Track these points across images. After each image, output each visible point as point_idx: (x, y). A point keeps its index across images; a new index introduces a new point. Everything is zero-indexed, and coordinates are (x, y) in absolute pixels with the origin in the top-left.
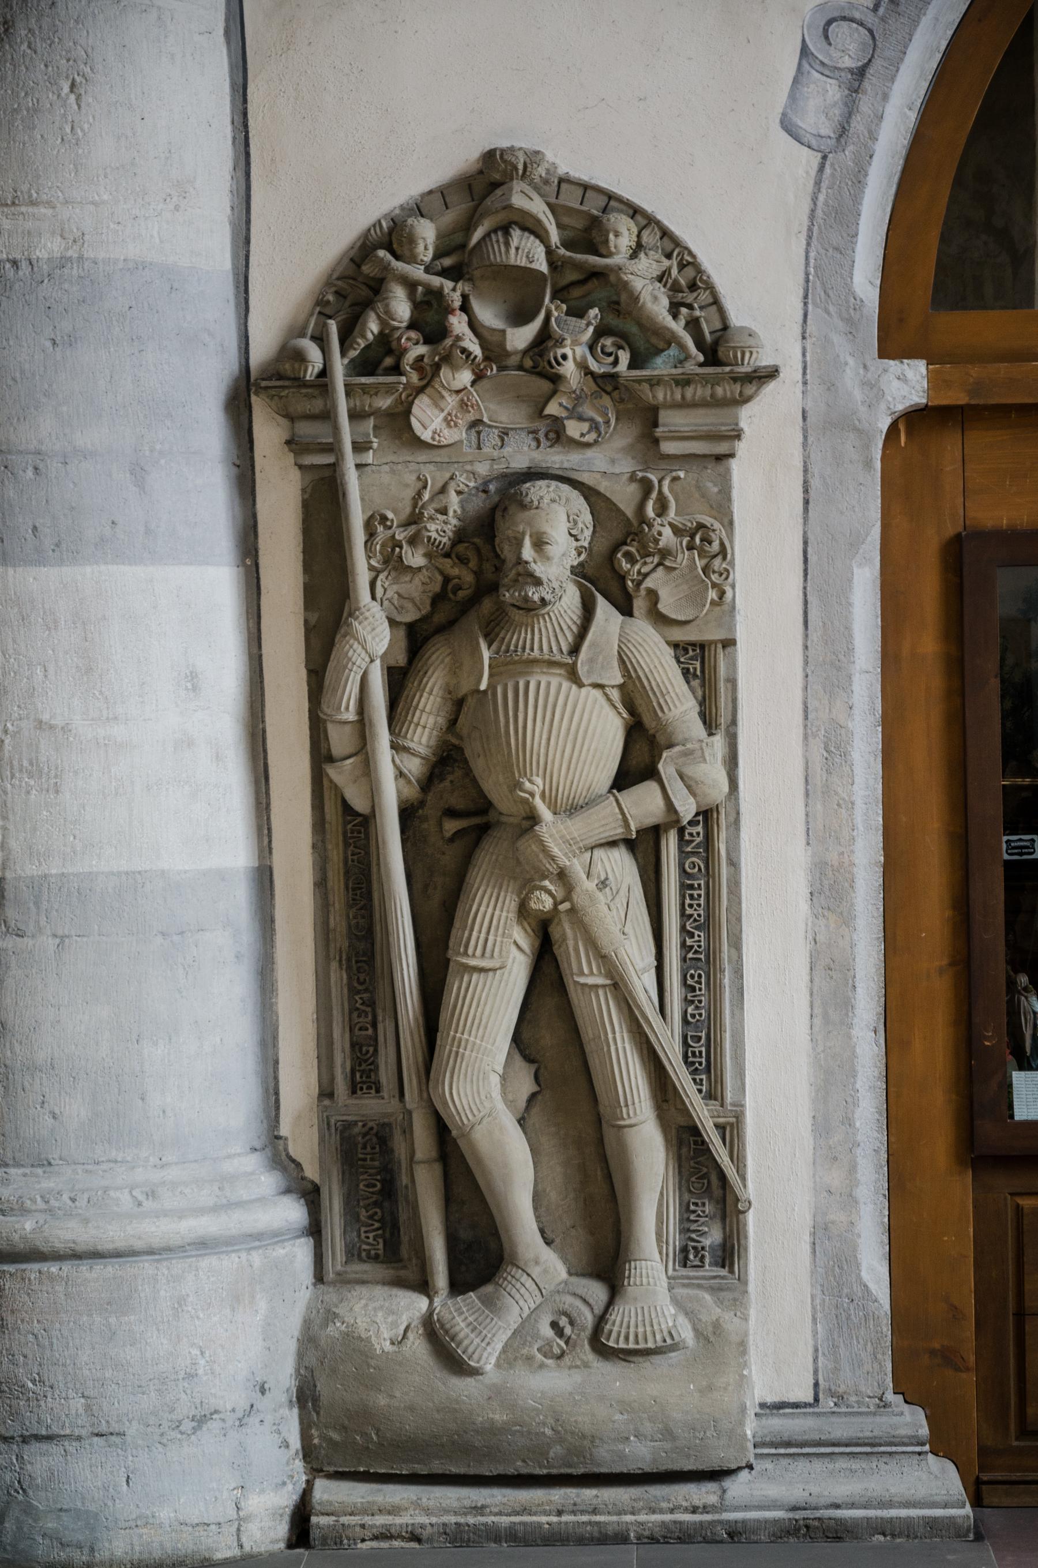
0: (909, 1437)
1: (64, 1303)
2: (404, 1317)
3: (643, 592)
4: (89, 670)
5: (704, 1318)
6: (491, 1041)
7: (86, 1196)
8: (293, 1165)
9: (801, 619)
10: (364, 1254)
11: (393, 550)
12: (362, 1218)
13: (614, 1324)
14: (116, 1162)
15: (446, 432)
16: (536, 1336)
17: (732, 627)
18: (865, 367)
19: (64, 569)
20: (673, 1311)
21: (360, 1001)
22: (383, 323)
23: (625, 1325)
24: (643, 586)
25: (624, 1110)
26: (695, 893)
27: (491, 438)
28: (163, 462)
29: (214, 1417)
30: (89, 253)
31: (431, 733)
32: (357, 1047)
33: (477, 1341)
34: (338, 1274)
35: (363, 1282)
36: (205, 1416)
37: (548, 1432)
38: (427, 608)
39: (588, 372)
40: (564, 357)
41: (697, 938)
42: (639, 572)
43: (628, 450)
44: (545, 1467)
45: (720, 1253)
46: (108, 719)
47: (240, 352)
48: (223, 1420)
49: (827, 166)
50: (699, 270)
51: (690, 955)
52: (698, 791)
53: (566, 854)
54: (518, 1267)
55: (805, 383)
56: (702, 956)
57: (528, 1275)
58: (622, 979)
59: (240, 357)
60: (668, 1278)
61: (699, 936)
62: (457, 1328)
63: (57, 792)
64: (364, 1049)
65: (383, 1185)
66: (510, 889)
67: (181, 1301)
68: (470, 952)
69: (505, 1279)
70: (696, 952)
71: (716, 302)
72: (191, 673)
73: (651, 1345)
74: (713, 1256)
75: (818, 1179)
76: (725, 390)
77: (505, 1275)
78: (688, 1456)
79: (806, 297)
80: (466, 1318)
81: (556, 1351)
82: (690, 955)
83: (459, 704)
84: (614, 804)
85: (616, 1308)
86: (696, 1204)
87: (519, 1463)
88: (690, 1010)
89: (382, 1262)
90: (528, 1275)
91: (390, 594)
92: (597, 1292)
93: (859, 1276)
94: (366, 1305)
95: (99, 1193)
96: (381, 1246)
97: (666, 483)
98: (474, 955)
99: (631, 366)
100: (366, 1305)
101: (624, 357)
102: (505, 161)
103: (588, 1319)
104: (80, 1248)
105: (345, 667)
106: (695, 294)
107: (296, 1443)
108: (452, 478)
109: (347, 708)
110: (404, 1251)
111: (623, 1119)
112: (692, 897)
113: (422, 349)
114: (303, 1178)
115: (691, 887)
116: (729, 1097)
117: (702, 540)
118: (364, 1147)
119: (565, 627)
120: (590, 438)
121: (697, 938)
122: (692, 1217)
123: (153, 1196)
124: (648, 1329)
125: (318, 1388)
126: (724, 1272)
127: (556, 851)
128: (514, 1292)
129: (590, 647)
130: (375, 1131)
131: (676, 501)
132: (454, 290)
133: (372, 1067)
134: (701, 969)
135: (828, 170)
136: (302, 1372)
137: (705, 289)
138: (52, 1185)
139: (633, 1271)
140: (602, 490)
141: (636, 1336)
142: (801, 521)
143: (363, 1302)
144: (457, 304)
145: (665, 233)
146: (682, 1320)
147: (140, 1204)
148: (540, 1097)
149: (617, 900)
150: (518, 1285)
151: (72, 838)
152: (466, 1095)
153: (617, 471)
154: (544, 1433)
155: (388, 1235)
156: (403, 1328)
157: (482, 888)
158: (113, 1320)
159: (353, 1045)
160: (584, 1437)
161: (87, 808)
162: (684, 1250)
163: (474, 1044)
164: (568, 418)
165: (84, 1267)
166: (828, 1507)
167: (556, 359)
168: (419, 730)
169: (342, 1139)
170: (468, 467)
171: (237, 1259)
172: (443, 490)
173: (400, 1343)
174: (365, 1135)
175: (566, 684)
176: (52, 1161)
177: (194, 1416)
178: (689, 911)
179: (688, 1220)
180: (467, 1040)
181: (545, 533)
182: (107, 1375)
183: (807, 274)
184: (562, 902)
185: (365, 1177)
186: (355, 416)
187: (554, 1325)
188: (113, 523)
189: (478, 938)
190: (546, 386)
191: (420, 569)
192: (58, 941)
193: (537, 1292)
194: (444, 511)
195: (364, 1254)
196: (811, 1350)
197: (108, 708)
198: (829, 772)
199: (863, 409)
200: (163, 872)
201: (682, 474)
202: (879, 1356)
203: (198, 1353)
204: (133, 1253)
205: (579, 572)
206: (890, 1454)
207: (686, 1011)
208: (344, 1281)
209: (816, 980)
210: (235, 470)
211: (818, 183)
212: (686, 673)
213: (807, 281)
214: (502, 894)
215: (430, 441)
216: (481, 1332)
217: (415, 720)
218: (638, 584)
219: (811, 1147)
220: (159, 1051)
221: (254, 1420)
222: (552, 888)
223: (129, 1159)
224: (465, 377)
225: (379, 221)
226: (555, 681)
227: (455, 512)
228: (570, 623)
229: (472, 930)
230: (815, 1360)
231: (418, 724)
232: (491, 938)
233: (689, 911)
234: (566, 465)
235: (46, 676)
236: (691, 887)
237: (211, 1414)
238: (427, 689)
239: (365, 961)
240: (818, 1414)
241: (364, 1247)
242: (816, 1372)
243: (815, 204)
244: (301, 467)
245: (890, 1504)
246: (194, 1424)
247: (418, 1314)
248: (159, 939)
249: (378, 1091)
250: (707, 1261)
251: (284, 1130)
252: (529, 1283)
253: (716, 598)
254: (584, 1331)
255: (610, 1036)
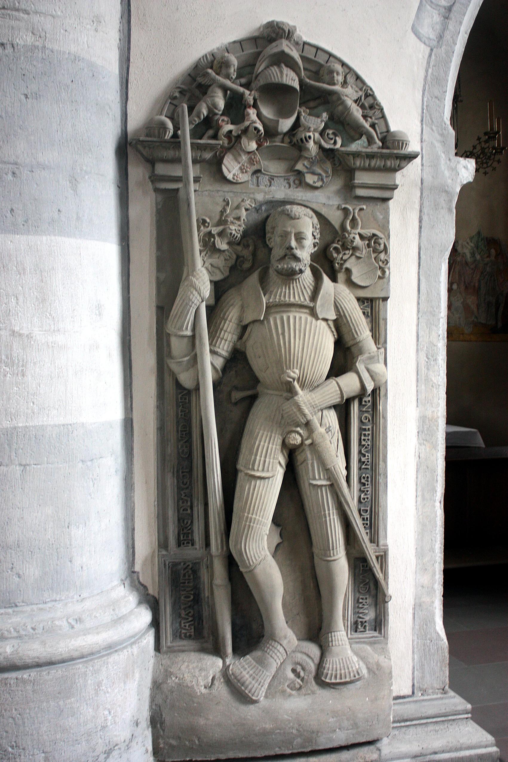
0: (463, 710)
1: (32, 696)
2: (211, 672)
3: (343, 270)
4: (44, 300)
5: (371, 660)
6: (267, 518)
7: (41, 625)
8: (142, 588)
9: (417, 289)
10: (183, 635)
11: (210, 240)
12: (183, 615)
13: (328, 670)
14: (56, 601)
15: (241, 175)
16: (286, 679)
17: (388, 291)
18: (449, 160)
19: (30, 237)
20: (356, 659)
21: (183, 495)
22: (210, 111)
23: (334, 669)
24: (344, 266)
25: (332, 552)
26: (367, 433)
27: (264, 180)
28: (87, 177)
29: (116, 748)
30: (49, 45)
31: (229, 344)
32: (181, 521)
33: (256, 685)
34: (169, 647)
35: (183, 651)
36: (111, 749)
37: (294, 731)
38: (227, 273)
39: (321, 147)
40: (310, 137)
41: (367, 457)
42: (342, 258)
43: (338, 192)
44: (291, 750)
45: (373, 624)
46: (54, 330)
47: (122, 122)
48: (120, 749)
49: (433, 54)
50: (375, 98)
51: (363, 467)
52: (376, 379)
53: (311, 413)
54: (275, 641)
55: (422, 165)
56: (369, 467)
57: (281, 645)
58: (336, 481)
59: (122, 125)
60: (349, 639)
61: (368, 456)
62: (245, 679)
63: (23, 375)
64: (185, 522)
65: (194, 597)
66: (277, 432)
67: (99, 684)
68: (256, 468)
69: (269, 648)
70: (366, 465)
71: (383, 117)
72: (98, 305)
73: (348, 679)
74: (370, 625)
75: (417, 581)
76: (391, 164)
77: (268, 645)
78: (363, 736)
79: (422, 121)
80: (248, 672)
81: (298, 686)
82: (363, 467)
83: (244, 328)
84: (336, 385)
85: (328, 660)
86: (362, 599)
87: (277, 749)
88: (362, 496)
89: (193, 639)
90: (281, 645)
91: (206, 265)
92: (314, 650)
93: (435, 628)
94: (188, 666)
95: (49, 623)
96: (193, 630)
97: (357, 211)
98: (258, 470)
99: (341, 146)
100: (188, 666)
101: (339, 141)
102: (279, 28)
103: (312, 667)
104: (41, 661)
105: (187, 304)
106: (373, 111)
107: (150, 748)
108: (243, 201)
109: (187, 328)
110: (206, 632)
111: (330, 556)
112: (365, 435)
113: (230, 127)
114: (148, 594)
115: (365, 430)
116: (381, 542)
117: (374, 243)
118: (184, 575)
119: (306, 287)
120: (319, 184)
121: (367, 457)
122: (361, 606)
123: (80, 622)
124: (347, 671)
125: (163, 717)
126: (376, 634)
127: (307, 411)
128: (273, 655)
129: (321, 299)
130: (190, 566)
131: (362, 222)
132: (250, 95)
133: (190, 531)
134: (368, 473)
135: (433, 57)
136: (154, 707)
137: (379, 109)
138: (19, 619)
139: (333, 638)
140: (323, 213)
141: (341, 675)
142: (417, 237)
143: (186, 664)
144: (252, 103)
145: (358, 78)
146: (361, 663)
147: (73, 627)
148: (282, 545)
149: (334, 438)
150: (276, 651)
151: (32, 404)
152: (253, 549)
153: (331, 203)
154: (292, 733)
155: (196, 624)
156: (211, 678)
157: (261, 432)
158: (61, 703)
159: (179, 520)
160: (313, 732)
161: (41, 386)
162: (356, 623)
163: (258, 520)
164: (307, 173)
165: (44, 671)
166: (431, 754)
167: (305, 138)
168: (223, 341)
169: (172, 572)
170: (252, 196)
171: (127, 653)
172: (238, 207)
173: (210, 687)
174: (185, 569)
175: (309, 318)
176: (18, 604)
177: (105, 751)
178: (363, 443)
179: (358, 607)
180: (255, 519)
181: (303, 233)
182: (58, 737)
183: (423, 109)
184: (307, 439)
185: (185, 592)
186: (195, 162)
187: (294, 671)
188: (59, 211)
189: (260, 460)
190: (296, 153)
191: (224, 251)
192: (22, 468)
193: (285, 654)
194: (238, 219)
195: (183, 635)
196: (411, 668)
197: (54, 324)
198: (428, 369)
199: (450, 181)
200: (83, 424)
201: (365, 207)
202: (443, 668)
203: (108, 713)
204: (72, 659)
205: (314, 257)
206: (454, 720)
207: (360, 497)
208: (171, 650)
209: (419, 477)
210: (118, 188)
211: (428, 63)
212: (364, 313)
213: (423, 113)
214: (273, 435)
215: (232, 180)
216: (258, 680)
217: (221, 336)
218: (342, 265)
219: (415, 564)
220: (80, 532)
221: (134, 744)
222: (301, 431)
223: (63, 598)
224: (253, 146)
225: (206, 55)
226: (304, 316)
227: (244, 220)
228: (309, 284)
229: (256, 455)
230: (413, 673)
231: (222, 339)
232: (267, 460)
233: (363, 443)
234: (304, 198)
235: (17, 303)
236: (365, 430)
237: (114, 747)
238: (229, 319)
239: (187, 472)
240: (416, 701)
241: (183, 631)
242: (413, 679)
243: (427, 73)
244: (156, 190)
245: (461, 749)
246: (106, 755)
247: (218, 670)
248: (80, 465)
249: (193, 545)
250: (367, 628)
251: (138, 567)
252: (281, 650)
253: (381, 275)
254: (311, 673)
255: (327, 512)
